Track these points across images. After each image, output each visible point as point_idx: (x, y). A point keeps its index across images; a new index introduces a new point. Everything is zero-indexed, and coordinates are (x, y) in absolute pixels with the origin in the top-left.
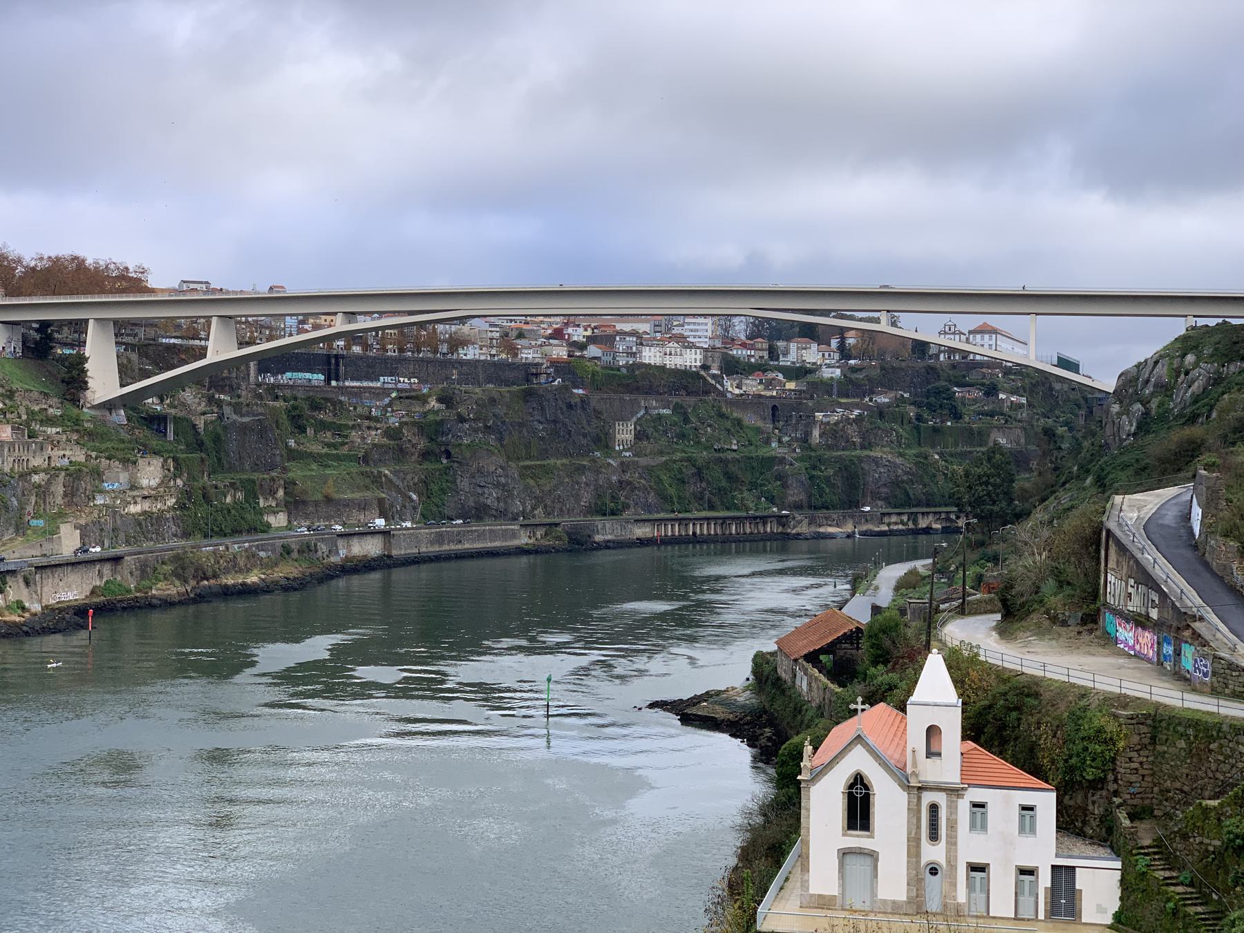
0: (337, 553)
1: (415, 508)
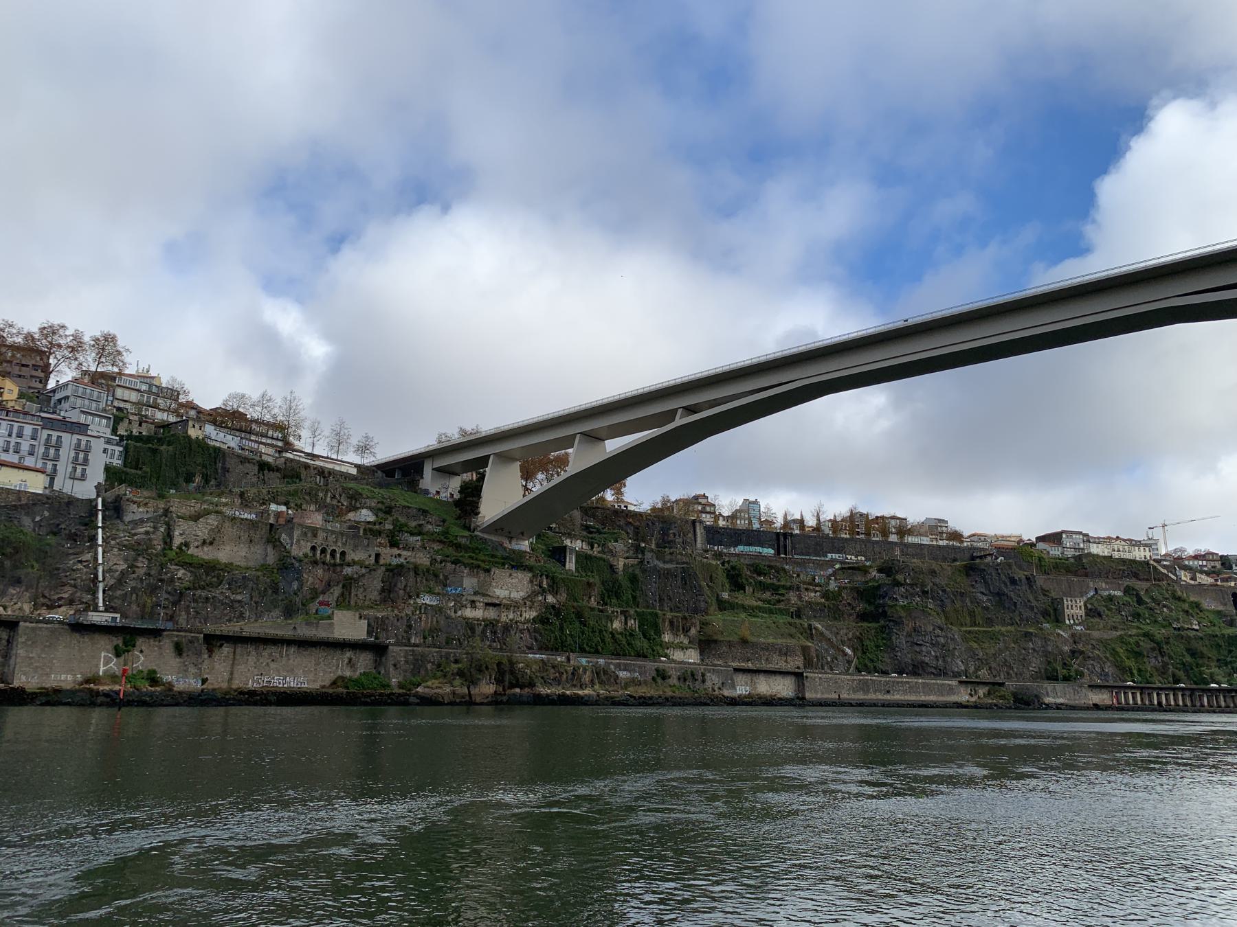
0: (734, 687)
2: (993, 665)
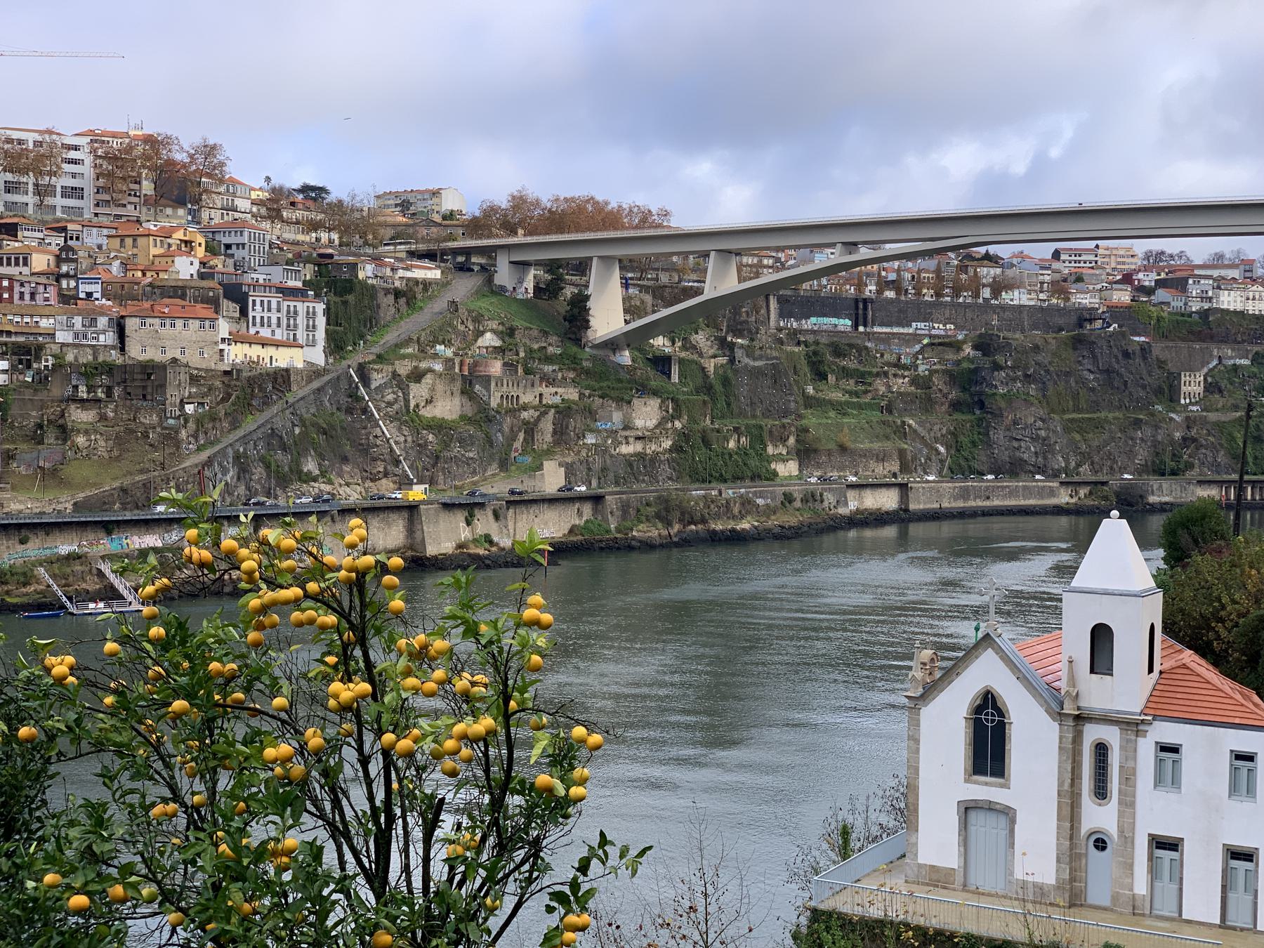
0: (846, 504)
1: (942, 461)
2: (1096, 459)
